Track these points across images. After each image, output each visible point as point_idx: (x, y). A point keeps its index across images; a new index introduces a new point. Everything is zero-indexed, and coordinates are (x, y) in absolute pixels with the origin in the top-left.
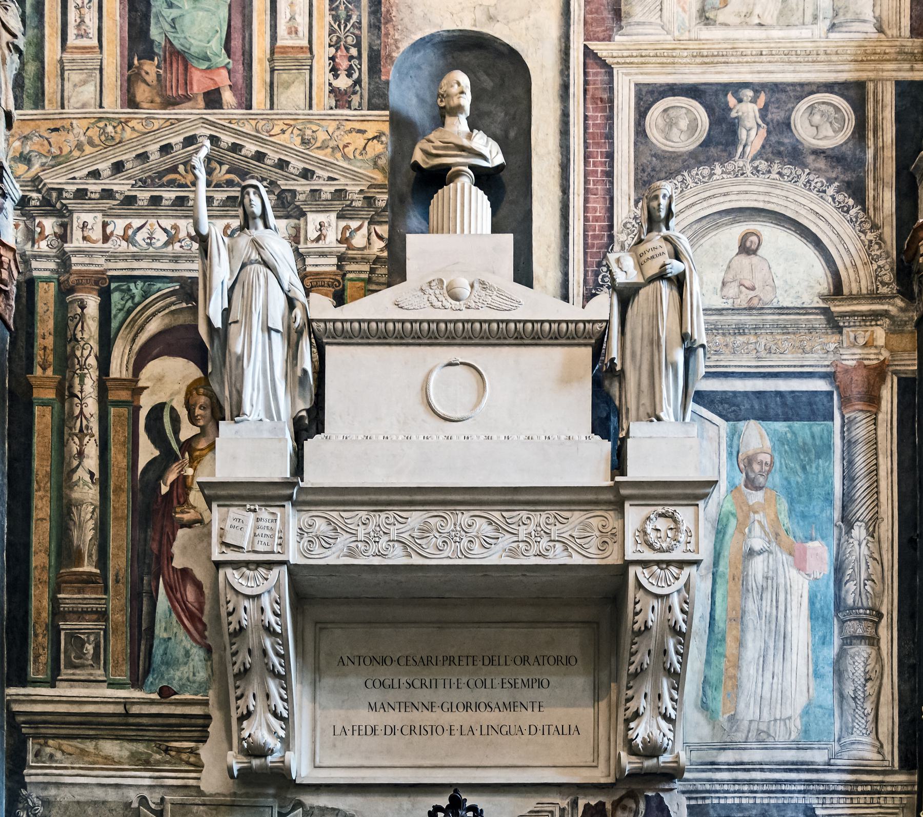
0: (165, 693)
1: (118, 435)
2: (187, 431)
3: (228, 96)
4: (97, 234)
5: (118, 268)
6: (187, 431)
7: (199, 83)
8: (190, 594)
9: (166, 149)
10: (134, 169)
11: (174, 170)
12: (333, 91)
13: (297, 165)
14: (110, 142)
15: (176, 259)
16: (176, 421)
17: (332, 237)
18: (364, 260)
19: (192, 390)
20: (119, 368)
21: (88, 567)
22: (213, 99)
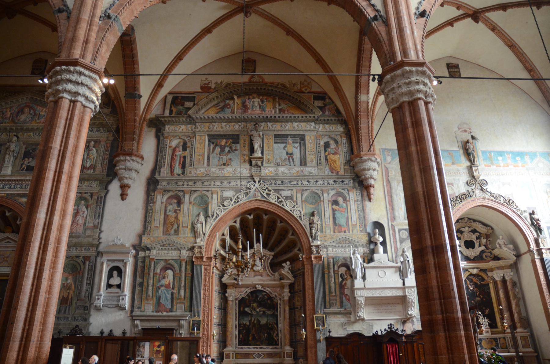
2: (345, 277)
3: (347, 231)
4: (331, 251)
5: (335, 255)
6: (345, 277)
7: (343, 229)
8: (348, 297)
9: (339, 239)
10: (335, 242)
12: (360, 230)
13: (357, 241)
14: (332, 238)
15: (342, 254)
16: (344, 275)
17: (362, 251)
19: (346, 271)
20: (336, 269)
21: (334, 294)
22: (345, 232)
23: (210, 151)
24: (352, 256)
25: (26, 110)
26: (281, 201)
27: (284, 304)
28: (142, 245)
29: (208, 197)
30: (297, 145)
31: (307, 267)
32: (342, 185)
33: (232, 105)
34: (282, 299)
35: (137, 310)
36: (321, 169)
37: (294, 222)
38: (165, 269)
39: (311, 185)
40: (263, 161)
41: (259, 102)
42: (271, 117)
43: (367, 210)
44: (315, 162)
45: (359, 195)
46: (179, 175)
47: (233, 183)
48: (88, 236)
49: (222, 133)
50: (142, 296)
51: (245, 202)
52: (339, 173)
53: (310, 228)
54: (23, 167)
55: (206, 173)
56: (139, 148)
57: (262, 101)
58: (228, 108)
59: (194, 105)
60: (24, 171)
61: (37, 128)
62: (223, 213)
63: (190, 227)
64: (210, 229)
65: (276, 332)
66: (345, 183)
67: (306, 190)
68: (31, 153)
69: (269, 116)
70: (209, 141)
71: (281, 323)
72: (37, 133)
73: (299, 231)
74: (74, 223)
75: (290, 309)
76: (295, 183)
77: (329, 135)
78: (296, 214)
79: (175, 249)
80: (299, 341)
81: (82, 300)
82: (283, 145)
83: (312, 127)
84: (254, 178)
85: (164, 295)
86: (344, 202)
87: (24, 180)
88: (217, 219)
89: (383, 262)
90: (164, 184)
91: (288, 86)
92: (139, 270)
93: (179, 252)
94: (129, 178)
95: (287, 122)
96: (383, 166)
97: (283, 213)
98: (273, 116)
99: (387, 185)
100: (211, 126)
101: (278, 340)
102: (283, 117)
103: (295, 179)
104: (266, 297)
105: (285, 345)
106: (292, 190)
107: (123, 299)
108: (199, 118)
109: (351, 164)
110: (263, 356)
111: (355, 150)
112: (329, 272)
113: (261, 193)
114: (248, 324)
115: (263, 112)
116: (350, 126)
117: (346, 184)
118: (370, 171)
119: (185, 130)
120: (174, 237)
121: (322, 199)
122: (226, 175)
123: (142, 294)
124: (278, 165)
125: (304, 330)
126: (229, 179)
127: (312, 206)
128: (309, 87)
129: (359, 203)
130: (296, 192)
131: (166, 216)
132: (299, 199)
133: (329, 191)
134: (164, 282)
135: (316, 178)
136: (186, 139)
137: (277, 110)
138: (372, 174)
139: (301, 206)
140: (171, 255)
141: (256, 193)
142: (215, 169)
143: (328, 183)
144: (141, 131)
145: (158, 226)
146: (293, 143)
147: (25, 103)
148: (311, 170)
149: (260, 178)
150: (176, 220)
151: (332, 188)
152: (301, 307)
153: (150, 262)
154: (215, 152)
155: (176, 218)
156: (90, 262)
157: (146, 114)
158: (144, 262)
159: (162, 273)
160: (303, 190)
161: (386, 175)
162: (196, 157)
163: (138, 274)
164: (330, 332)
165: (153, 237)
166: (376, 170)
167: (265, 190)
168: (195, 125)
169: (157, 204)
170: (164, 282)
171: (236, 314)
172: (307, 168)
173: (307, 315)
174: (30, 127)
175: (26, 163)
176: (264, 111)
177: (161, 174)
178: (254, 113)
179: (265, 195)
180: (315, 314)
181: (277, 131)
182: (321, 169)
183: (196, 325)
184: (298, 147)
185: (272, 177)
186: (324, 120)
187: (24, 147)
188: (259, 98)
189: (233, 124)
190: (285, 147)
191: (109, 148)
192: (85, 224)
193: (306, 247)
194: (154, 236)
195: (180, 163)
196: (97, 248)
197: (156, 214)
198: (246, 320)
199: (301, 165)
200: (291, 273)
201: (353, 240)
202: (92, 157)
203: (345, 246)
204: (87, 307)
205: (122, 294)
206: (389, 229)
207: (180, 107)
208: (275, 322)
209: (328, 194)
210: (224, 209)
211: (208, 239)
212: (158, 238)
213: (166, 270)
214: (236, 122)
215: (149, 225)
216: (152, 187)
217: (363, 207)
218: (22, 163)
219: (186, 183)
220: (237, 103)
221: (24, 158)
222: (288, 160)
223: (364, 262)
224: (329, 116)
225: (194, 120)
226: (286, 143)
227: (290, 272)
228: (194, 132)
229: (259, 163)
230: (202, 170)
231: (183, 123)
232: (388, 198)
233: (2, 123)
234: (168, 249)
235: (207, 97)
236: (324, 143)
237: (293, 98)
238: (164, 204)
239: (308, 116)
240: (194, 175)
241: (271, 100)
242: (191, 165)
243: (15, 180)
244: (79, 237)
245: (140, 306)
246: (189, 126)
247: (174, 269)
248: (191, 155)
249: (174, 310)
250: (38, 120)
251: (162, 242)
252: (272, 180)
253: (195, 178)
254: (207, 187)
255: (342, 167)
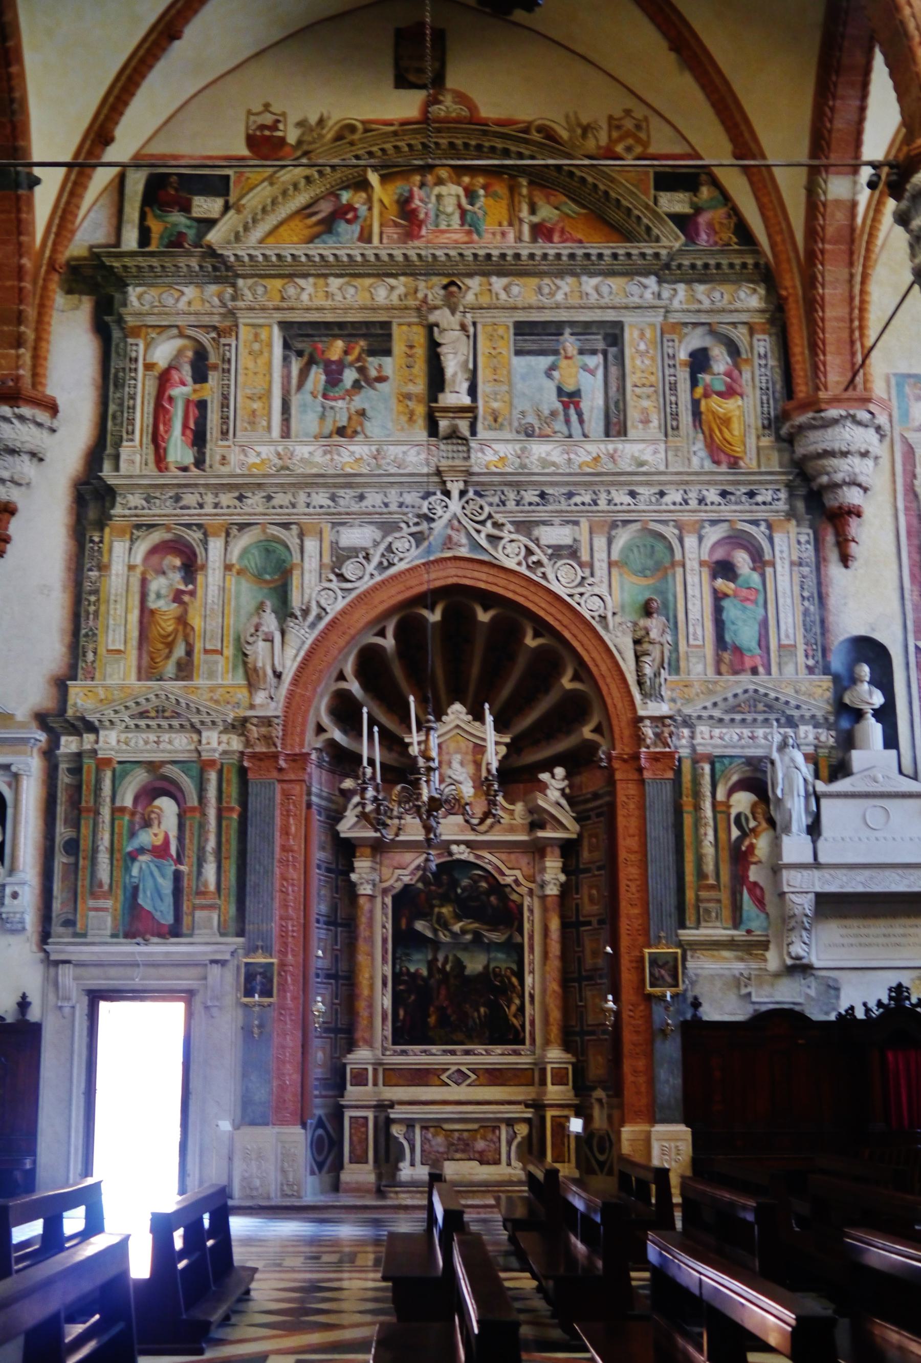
0: (749, 932)
1: (722, 826)
4: (707, 736)
5: (718, 752)
6: (752, 824)
7: (748, 663)
8: (758, 892)
9: (736, 696)
10: (721, 705)
11: (739, 706)
12: (808, 667)
13: (793, 703)
14: (711, 692)
15: (743, 747)
16: (747, 819)
17: (811, 737)
18: (826, 747)
20: (721, 795)
21: (711, 881)
22: (754, 671)
23: (289, 382)
24: (775, 756)
26: (539, 563)
27: (545, 910)
28: (70, 712)
29: (287, 547)
30: (595, 361)
31: (625, 792)
32: (747, 507)
33: (363, 210)
34: (537, 892)
35: (61, 930)
36: (677, 449)
37: (581, 636)
38: (149, 794)
39: (642, 507)
40: (475, 418)
41: (458, 196)
42: (503, 256)
43: (833, 601)
44: (655, 423)
45: (808, 542)
46: (185, 469)
47: (374, 499)
49: (329, 317)
50: (76, 885)
51: (418, 566)
52: (741, 463)
53: (637, 657)
55: (279, 463)
56: (40, 370)
57: (471, 195)
58: (349, 222)
59: (227, 208)
62: (341, 604)
63: (229, 651)
64: (299, 659)
65: (517, 1001)
66: (759, 499)
67: (626, 522)
69: (495, 253)
70: (286, 346)
71: (532, 972)
73: (599, 667)
75: (565, 926)
76: (587, 499)
77: (709, 324)
78: (588, 607)
79: (182, 726)
80: (593, 1033)
82: (544, 362)
83: (648, 295)
84: (444, 482)
85: (150, 883)
86: (754, 569)
88: (322, 625)
89: (880, 777)
90: (135, 500)
91: (565, 134)
92: (62, 797)
93: (195, 737)
94: (12, 481)
95: (561, 274)
96: (897, 438)
97: (543, 605)
98: (510, 252)
99: (907, 509)
100: (291, 291)
101: (523, 1026)
102: (545, 256)
103: (585, 484)
104: (484, 884)
105: (547, 1043)
106: (576, 523)
107: (15, 895)
108: (246, 259)
109: (784, 431)
110: (473, 1077)
111: (800, 381)
112: (697, 808)
113: (469, 535)
114: (424, 972)
115: (475, 237)
116: (784, 293)
117: (764, 503)
118: (850, 460)
119: (197, 307)
120: (174, 687)
121: (678, 556)
122: (349, 470)
123: (76, 879)
124: (528, 435)
125: (610, 997)
126: (358, 485)
127: (644, 582)
128: (638, 140)
129: (806, 570)
130: (591, 533)
131: (147, 615)
132: (601, 556)
133: (703, 527)
134: (146, 838)
135: (660, 483)
136: (205, 339)
137: (526, 229)
138: (857, 470)
139: (606, 580)
140: (169, 747)
141: (453, 534)
142: (311, 448)
143: (701, 501)
144: (43, 309)
145: (122, 648)
146: (581, 352)
148: (642, 451)
149: (465, 482)
150: (181, 628)
151: (714, 516)
152: (601, 922)
153: (98, 770)
154: (309, 385)
155: (182, 620)
157: (55, 244)
158: (76, 771)
159: (139, 809)
160: (614, 525)
161: (904, 470)
162: (240, 402)
163: (61, 810)
164: (696, 1004)
165: (106, 688)
166: (872, 455)
167: (482, 523)
168: (234, 285)
169: (113, 572)
170: (146, 838)
171: (384, 941)
172: (628, 446)
173: (623, 950)
176: (479, 234)
177: (123, 465)
178: (443, 239)
179: (484, 542)
180: (649, 947)
181: (524, 308)
182: (677, 449)
183: (259, 978)
184: (597, 367)
185: (510, 478)
186: (693, 266)
188: (459, 184)
189: (368, 281)
190: (553, 367)
193: (621, 725)
194: (108, 682)
195: (185, 426)
197: (112, 606)
198: (419, 961)
199: (607, 434)
200: (567, 807)
201: (783, 699)
203: (755, 720)
205: (9, 880)
206: (907, 664)
207: (177, 218)
208: (514, 967)
209: (701, 539)
210: (342, 589)
211: (291, 695)
212: (122, 688)
213: (154, 798)
214: (377, 276)
215: (91, 646)
216: (92, 514)
217: (819, 584)
219: (209, 499)
220: (381, 201)
222: (561, 417)
223: (817, 776)
224: (712, 253)
225: (229, 268)
226: (556, 352)
227: (563, 802)
228: (231, 313)
229: (463, 426)
230: (266, 451)
231: (192, 278)
232: (909, 552)
234: (159, 726)
235: (271, 180)
236: (692, 355)
237: (583, 180)
238: (139, 571)
239: (635, 252)
240: (238, 471)
241: (501, 189)
242: (224, 434)
245: (71, 917)
246: (213, 289)
247: (179, 795)
248: (225, 397)
249: (185, 930)
251: (137, 703)
252: (505, 489)
253: (240, 481)
254: (287, 511)
255: (752, 442)
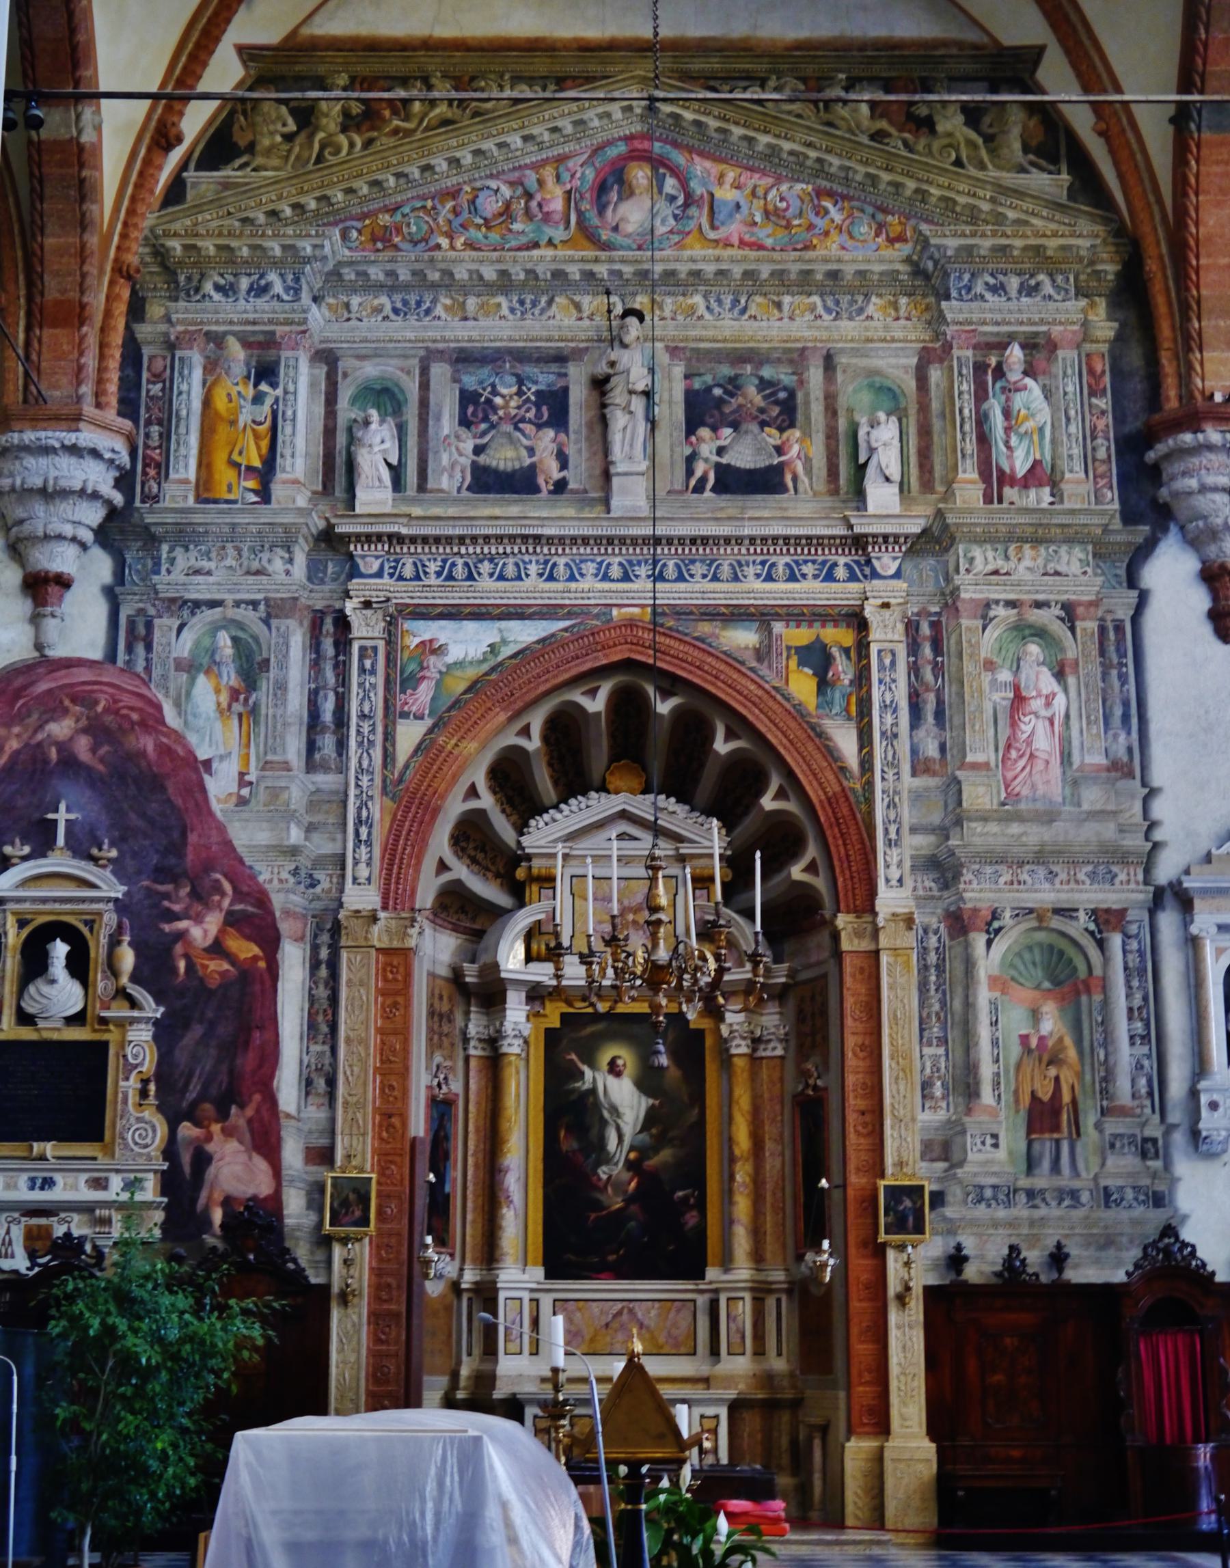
25: (640, 175)
48: (1094, 815)
54: (699, 473)
60: (708, 494)
61: (721, 273)
68: (720, 402)
72: (728, 300)
74: (1014, 754)
81: (1122, 1112)
87: (727, 540)
147: (629, 139)
156: (1127, 936)
174: (683, 269)
175: (707, 450)
187: (679, 370)
191: (1107, 379)
192: (1066, 757)
196: (1147, 871)
202: (1030, 425)
204: (1154, 1141)
218: (688, 451)
221: (691, 429)
233: (536, 245)
243: (681, 540)
244: (1049, 817)
250: (713, 227)
